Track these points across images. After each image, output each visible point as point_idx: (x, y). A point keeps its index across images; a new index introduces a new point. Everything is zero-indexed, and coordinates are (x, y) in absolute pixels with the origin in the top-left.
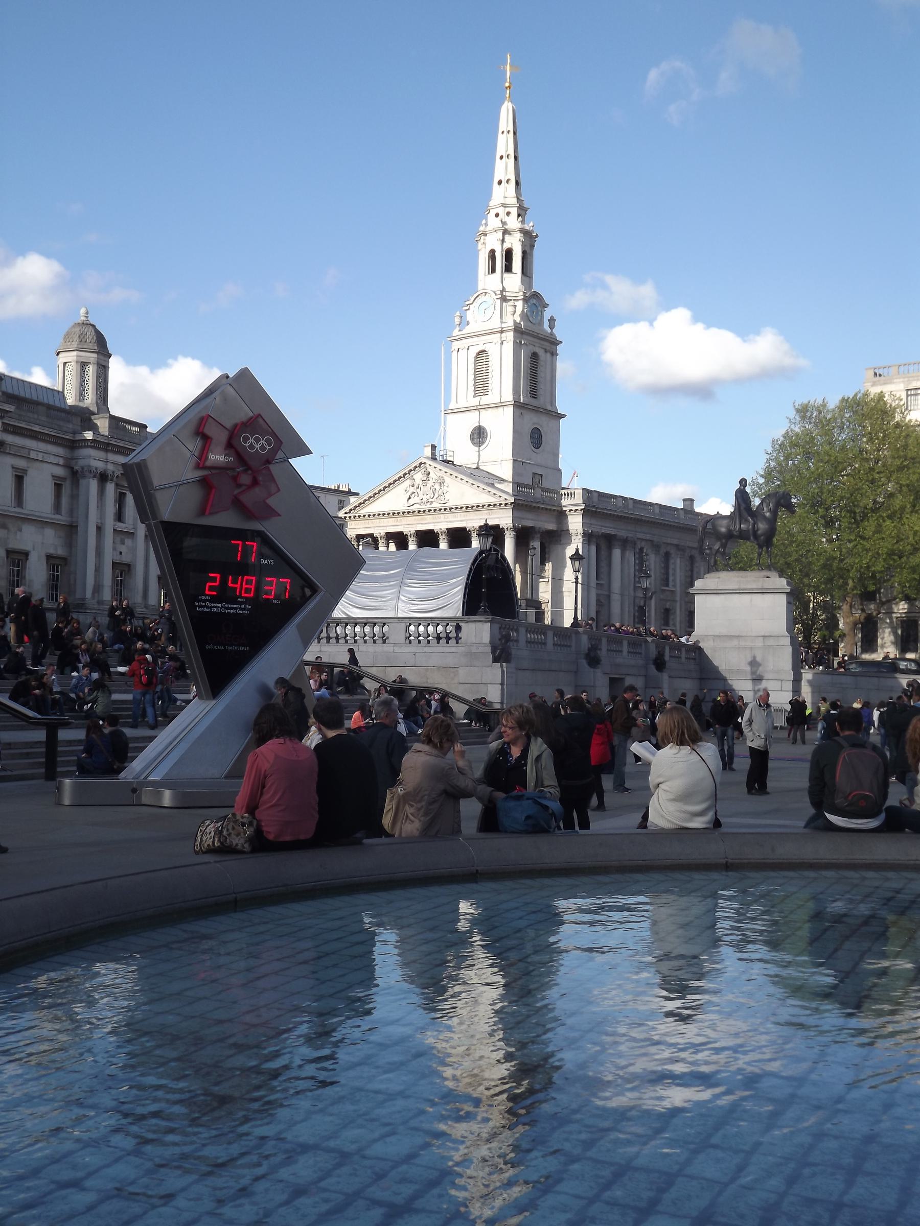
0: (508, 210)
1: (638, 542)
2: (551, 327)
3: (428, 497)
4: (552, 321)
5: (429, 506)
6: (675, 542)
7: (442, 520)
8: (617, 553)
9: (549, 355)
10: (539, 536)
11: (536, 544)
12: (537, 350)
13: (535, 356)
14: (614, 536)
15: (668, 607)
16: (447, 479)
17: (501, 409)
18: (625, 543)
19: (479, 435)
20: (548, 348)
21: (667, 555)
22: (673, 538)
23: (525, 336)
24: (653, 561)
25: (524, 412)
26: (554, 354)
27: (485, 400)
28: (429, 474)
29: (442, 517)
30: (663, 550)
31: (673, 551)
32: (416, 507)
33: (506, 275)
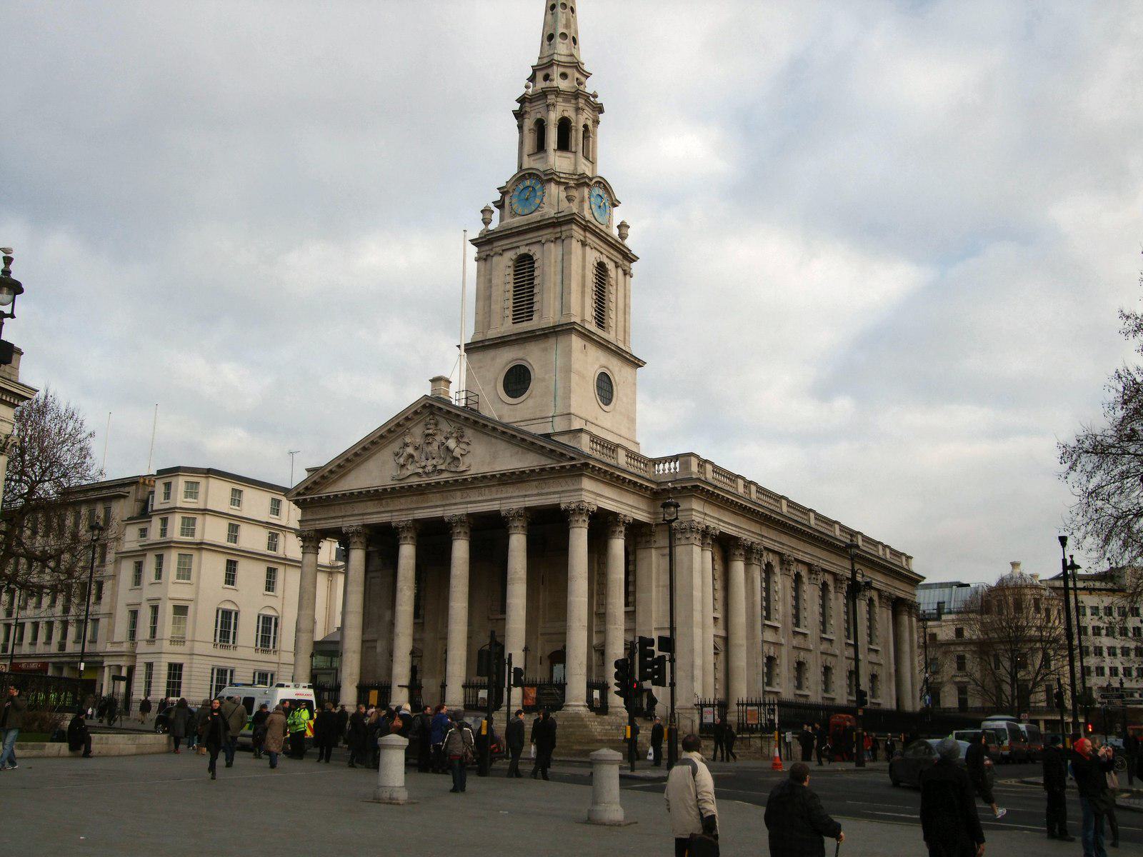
0: (561, 70)
1: (765, 554)
2: (623, 236)
3: (434, 462)
4: (623, 226)
5: (435, 478)
6: (807, 559)
7: (458, 500)
8: (739, 566)
9: (620, 271)
10: (623, 529)
11: (618, 546)
12: (606, 260)
13: (601, 267)
14: (736, 539)
15: (801, 660)
16: (469, 433)
17: (552, 341)
18: (750, 553)
19: (517, 381)
20: (621, 262)
21: (798, 579)
22: (806, 552)
23: (588, 235)
24: (782, 583)
25: (588, 345)
26: (626, 273)
27: (525, 326)
28: (436, 425)
29: (458, 497)
30: (794, 569)
31: (804, 573)
32: (415, 481)
33: (559, 153)
